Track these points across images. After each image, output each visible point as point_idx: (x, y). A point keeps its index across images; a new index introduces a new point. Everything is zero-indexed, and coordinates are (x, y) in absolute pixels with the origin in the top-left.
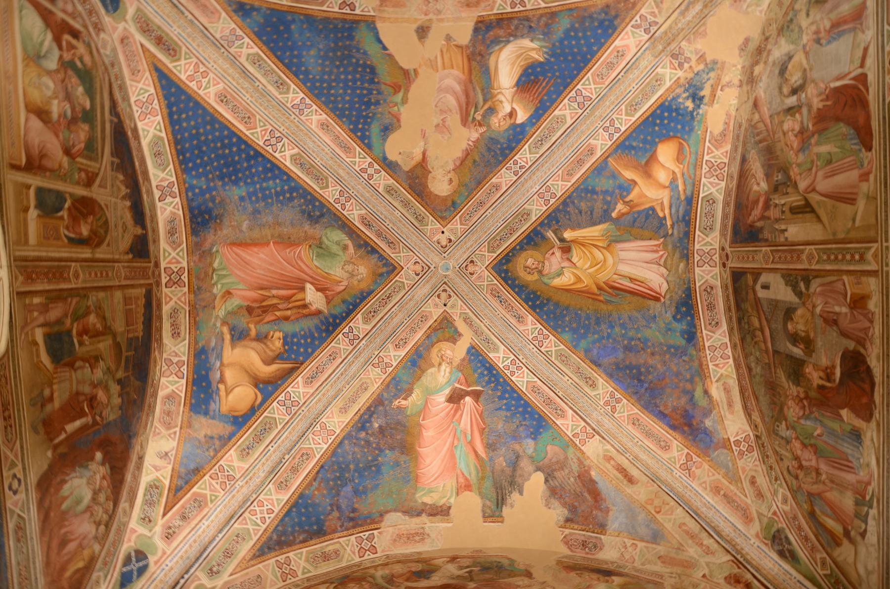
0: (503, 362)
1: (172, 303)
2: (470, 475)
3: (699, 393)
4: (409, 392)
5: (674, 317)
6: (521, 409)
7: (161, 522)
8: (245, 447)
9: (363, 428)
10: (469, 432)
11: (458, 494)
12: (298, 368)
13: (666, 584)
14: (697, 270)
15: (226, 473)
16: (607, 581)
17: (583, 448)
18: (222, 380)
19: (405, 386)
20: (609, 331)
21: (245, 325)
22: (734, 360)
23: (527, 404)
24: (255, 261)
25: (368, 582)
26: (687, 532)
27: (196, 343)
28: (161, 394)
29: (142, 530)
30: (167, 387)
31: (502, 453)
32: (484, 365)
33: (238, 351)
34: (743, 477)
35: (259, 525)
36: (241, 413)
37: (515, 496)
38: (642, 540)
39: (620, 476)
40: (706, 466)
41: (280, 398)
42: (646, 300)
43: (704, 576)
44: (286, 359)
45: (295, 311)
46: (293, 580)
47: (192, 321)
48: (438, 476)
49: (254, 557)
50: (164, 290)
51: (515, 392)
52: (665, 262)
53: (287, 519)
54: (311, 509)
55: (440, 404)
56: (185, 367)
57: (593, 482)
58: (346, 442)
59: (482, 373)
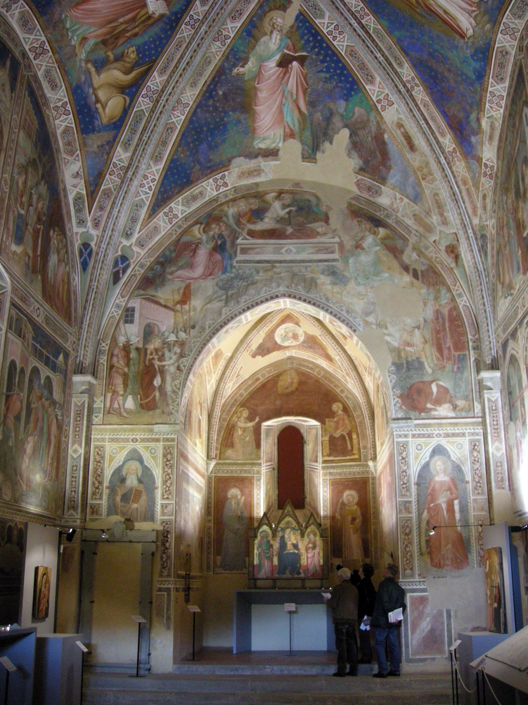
0: (328, 27)
1: (43, 68)
2: (294, 126)
3: (473, 116)
4: (245, 61)
5: (472, 56)
6: (338, 72)
7: (89, 219)
8: (126, 141)
9: (211, 97)
10: (295, 92)
11: (284, 140)
12: (152, 66)
13: (411, 240)
14: (499, 35)
15: (119, 166)
16: (375, 233)
17: (382, 113)
18: (98, 101)
19: (243, 55)
20: (420, 36)
21: (104, 55)
22: (504, 113)
23: (344, 67)
24: (99, 6)
25: (225, 223)
26: (437, 202)
27: (71, 85)
28: (59, 132)
29: (81, 230)
30: (61, 125)
31: (319, 109)
32: (309, 32)
33: (103, 76)
34: (481, 189)
35: (147, 193)
36: (117, 118)
37: (327, 144)
38: (407, 197)
39: (405, 142)
40: (463, 164)
41: (143, 93)
42: (453, 32)
43: (435, 242)
44: (142, 64)
45: (141, 27)
46: (176, 220)
47: (63, 72)
48: (270, 127)
49: (150, 216)
50: (34, 62)
51: (337, 56)
52: (476, 16)
53: (165, 181)
54: (180, 169)
55: (271, 69)
56: (69, 105)
57: (384, 143)
58: (199, 110)
59: (308, 40)
